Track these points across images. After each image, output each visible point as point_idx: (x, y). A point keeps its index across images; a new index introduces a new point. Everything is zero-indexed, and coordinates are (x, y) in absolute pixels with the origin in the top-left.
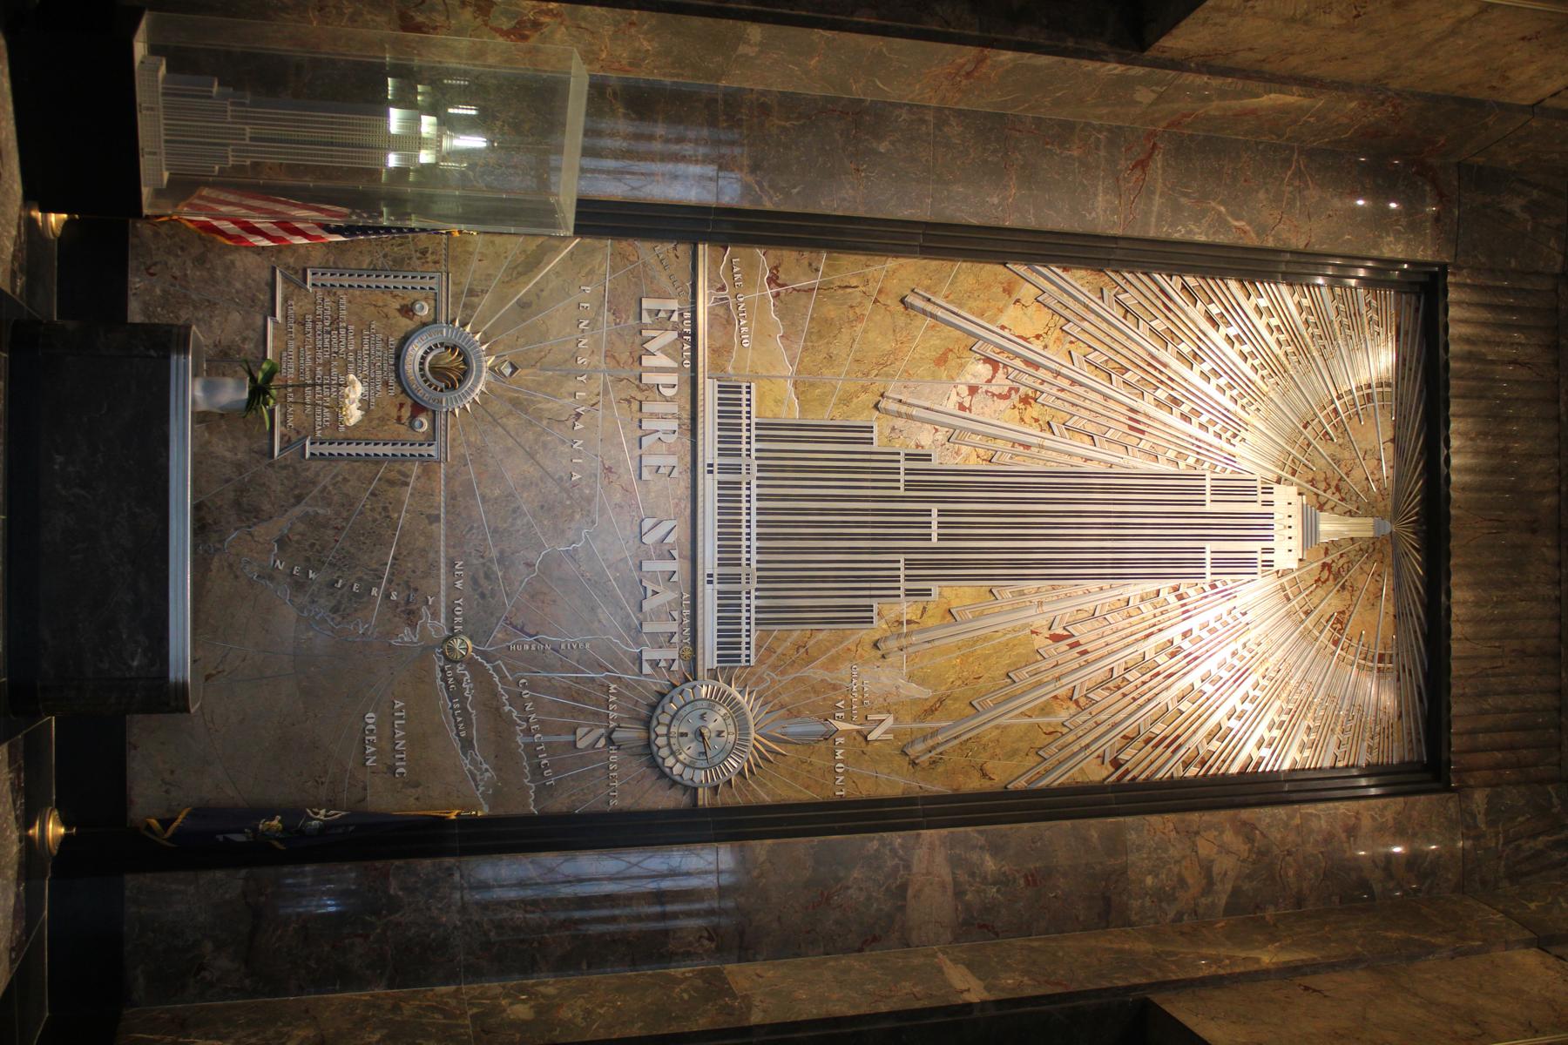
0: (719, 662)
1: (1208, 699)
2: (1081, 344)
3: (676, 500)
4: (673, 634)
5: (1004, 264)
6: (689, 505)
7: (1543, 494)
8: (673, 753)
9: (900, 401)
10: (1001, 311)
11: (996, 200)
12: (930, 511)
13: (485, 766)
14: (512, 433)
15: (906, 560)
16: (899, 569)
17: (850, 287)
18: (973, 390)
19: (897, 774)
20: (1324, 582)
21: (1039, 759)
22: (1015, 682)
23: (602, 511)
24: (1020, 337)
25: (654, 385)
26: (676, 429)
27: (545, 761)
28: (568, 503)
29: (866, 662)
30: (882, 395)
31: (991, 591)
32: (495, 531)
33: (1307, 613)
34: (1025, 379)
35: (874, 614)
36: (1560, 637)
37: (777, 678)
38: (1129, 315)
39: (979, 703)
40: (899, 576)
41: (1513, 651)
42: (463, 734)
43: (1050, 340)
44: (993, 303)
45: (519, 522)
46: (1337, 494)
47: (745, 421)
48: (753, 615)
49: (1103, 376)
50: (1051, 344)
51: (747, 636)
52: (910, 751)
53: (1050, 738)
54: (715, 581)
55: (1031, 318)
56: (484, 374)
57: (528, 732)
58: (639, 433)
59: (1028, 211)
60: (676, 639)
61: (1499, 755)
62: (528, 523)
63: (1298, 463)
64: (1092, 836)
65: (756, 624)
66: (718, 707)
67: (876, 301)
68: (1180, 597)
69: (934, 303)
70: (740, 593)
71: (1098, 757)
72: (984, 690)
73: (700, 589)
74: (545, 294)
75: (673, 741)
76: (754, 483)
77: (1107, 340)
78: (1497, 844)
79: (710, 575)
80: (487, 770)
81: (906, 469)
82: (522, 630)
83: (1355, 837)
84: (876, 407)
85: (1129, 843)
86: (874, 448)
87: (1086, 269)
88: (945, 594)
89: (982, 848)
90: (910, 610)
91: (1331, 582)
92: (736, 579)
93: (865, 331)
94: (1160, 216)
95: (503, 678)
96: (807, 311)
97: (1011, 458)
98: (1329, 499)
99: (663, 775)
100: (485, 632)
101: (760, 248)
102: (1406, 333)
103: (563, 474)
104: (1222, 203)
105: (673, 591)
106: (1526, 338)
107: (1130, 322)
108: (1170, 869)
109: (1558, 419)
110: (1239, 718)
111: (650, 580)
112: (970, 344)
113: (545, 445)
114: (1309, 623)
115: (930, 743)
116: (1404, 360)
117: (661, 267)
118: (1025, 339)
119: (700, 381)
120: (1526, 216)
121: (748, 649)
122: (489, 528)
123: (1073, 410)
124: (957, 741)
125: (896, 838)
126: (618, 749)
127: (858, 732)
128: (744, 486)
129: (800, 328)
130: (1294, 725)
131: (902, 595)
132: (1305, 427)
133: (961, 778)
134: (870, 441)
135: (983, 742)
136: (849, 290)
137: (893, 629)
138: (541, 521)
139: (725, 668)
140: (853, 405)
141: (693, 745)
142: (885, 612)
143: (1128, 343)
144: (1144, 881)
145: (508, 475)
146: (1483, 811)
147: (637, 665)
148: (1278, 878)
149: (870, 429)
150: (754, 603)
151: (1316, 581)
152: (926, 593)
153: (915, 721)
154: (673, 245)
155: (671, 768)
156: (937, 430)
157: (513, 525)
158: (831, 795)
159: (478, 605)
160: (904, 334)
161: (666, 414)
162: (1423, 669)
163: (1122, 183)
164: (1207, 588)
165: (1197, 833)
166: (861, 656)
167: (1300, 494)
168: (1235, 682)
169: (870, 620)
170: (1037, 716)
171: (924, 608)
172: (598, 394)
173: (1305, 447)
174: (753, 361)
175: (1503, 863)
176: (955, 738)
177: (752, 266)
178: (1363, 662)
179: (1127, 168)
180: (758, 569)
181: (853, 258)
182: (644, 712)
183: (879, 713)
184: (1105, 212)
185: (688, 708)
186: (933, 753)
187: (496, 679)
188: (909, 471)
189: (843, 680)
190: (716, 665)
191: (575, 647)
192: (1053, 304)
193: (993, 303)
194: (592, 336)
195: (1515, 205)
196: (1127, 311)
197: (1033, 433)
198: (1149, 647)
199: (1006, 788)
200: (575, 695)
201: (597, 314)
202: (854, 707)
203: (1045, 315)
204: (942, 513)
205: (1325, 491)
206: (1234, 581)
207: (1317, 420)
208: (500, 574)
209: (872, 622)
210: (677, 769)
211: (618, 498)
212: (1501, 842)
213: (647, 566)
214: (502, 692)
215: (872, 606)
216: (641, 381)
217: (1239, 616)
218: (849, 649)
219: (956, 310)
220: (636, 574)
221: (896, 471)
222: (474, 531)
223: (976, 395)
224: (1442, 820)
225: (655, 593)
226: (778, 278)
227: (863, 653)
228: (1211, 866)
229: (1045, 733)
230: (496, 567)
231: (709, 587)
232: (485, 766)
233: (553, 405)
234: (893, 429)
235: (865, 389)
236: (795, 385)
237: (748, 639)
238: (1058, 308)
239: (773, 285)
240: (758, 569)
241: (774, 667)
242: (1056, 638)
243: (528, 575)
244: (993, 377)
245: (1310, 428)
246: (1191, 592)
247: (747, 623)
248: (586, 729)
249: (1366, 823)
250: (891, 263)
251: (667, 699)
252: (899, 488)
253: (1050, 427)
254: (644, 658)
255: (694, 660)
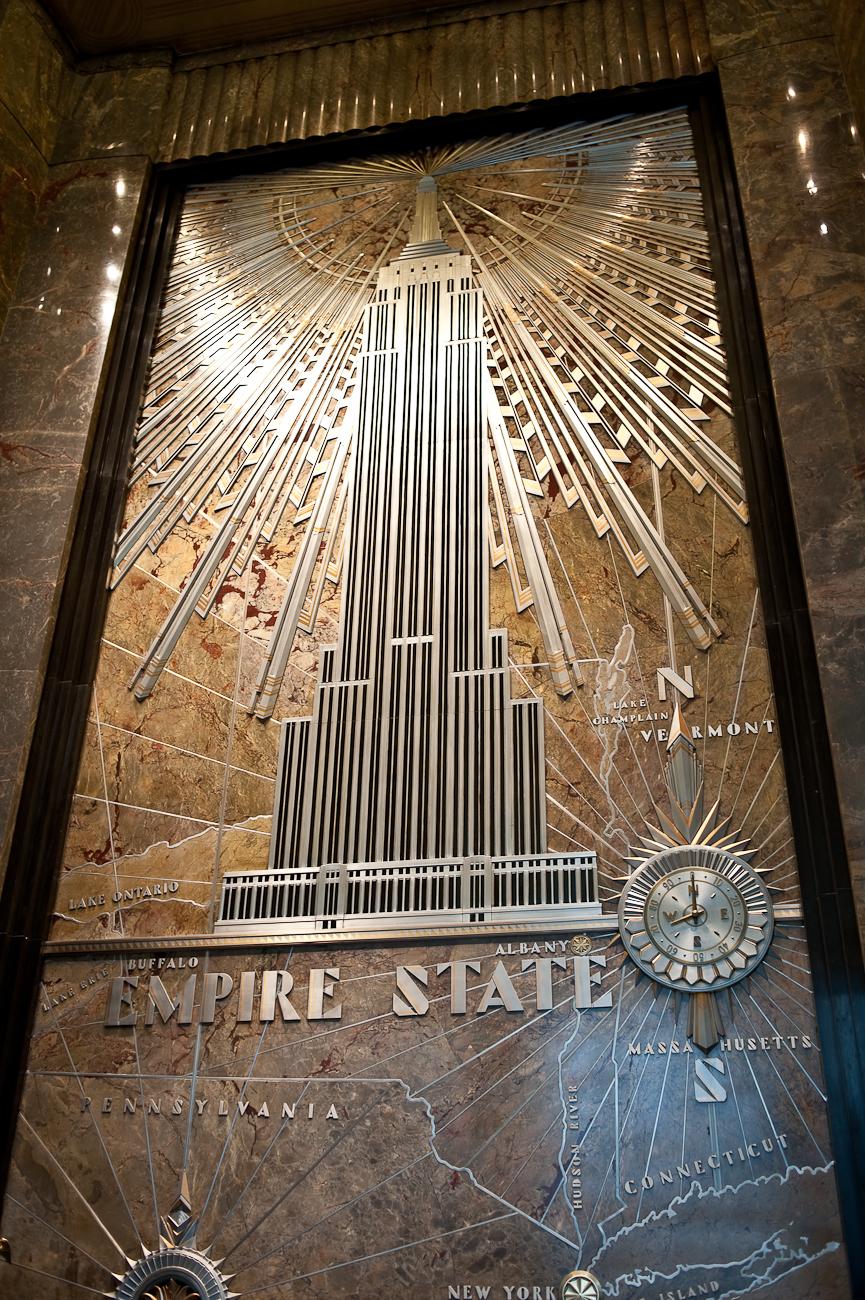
0: (592, 900)
1: (624, 322)
2: (209, 501)
3: (371, 969)
4: (556, 967)
5: (110, 591)
6: (378, 951)
7: (391, 49)
8: (726, 957)
9: (259, 694)
10: (163, 590)
11: (27, 598)
12: (394, 647)
13: (764, 1248)
14: (269, 1209)
15: (455, 670)
16: (467, 678)
17: (119, 763)
18: (252, 612)
19: (737, 656)
20: (487, 229)
21: (708, 493)
22: (610, 530)
23: (383, 1073)
24: (194, 568)
25: (217, 1006)
26: (276, 972)
27: (750, 1151)
28: (368, 1123)
29: (590, 709)
30: (250, 715)
31: (496, 568)
32: (405, 1233)
33: (522, 240)
34: (242, 556)
35: (525, 702)
36: (542, 9)
37: (613, 817)
38: (180, 456)
39: (638, 568)
40: (476, 677)
41: (557, 43)
42: (715, 1286)
43: (201, 533)
44: (154, 600)
45: (393, 1197)
46: (389, 231)
47: (272, 882)
48: (528, 856)
49: (247, 476)
50: (205, 533)
51: (555, 863)
52: (705, 644)
53: (680, 482)
54: (480, 910)
55: (175, 557)
56: (184, 1253)
57: (706, 1178)
58: (279, 1024)
59: (43, 563)
60: (561, 961)
61: (673, 37)
62: (395, 1183)
63: (354, 271)
64: (798, 410)
65: (539, 852)
66: (655, 897)
67: (138, 731)
68: (503, 365)
69: (147, 664)
70: (496, 877)
71: (700, 427)
72: (621, 564)
73: (491, 931)
74: (86, 1163)
75: (708, 958)
76: (351, 866)
77: (206, 474)
78: (772, 16)
79: (473, 918)
80: (770, 1245)
81: (342, 680)
82: (551, 1190)
83: (775, 144)
84: (264, 721)
85: (803, 369)
86: (313, 719)
87: (125, 505)
88: (499, 621)
89: (825, 535)
90: (520, 661)
91: (487, 223)
92: (477, 883)
93: (172, 741)
94: (67, 428)
95: (624, 1220)
96: (141, 812)
97: (334, 562)
98: (396, 238)
99: (757, 972)
100: (555, 1249)
101: (59, 876)
102: (225, 194)
103: (329, 1131)
104: (59, 369)
105: (493, 968)
106: (233, 87)
107: (188, 453)
108: (833, 320)
109: (315, 49)
110: (646, 287)
111: (478, 1001)
112: (198, 620)
113: (288, 1159)
114: (530, 238)
115: (693, 619)
116: (252, 192)
117: (68, 1002)
118: (198, 560)
119: (215, 943)
120: (109, 103)
121: (573, 861)
122: (400, 1243)
123: (283, 501)
124: (690, 589)
125: (822, 640)
126: (724, 1037)
127: (683, 709)
128: (354, 879)
129: (162, 820)
130: (652, 233)
131: (501, 671)
132: (316, 270)
133: (738, 579)
134: (306, 726)
135: (690, 558)
136: (122, 764)
137: (545, 678)
138: (393, 1163)
139: (600, 890)
140: (260, 749)
141: (712, 928)
142: (523, 691)
143: (211, 453)
144: (851, 345)
145: (325, 1213)
146: (735, 36)
147: (600, 1014)
148: (834, 209)
149: (291, 727)
150: (510, 856)
151: (486, 236)
152: (497, 643)
153: (666, 642)
154: (44, 987)
155: (748, 958)
156: (297, 648)
157: (396, 1206)
158: (773, 737)
159: (513, 1260)
160: (180, 695)
161: (256, 987)
162: (584, 125)
163: (25, 469)
164: (493, 339)
165: (784, 299)
166: (581, 714)
167: (388, 265)
168: (602, 297)
169: (533, 709)
170: (652, 500)
171: (517, 643)
172: (224, 1082)
173: (337, 267)
174: (196, 878)
175: (794, 7)
176: (685, 591)
177: (80, 885)
178: (576, 180)
179: (10, 465)
180: (465, 854)
181: (84, 762)
182: (667, 1001)
183: (656, 686)
184: (54, 483)
185: (659, 939)
186: (709, 617)
187: (627, 1229)
188: (345, 676)
189: (612, 736)
190: (596, 903)
191: (575, 1108)
192: (160, 535)
193: (154, 600)
194: (146, 1094)
195: (96, 113)
196: (176, 458)
197: (307, 543)
198: (562, 392)
199: (746, 525)
200: (646, 1105)
201: (119, 1086)
202: (649, 717)
203: (174, 543)
204: (397, 633)
205: (387, 242)
206: (485, 314)
207: (309, 260)
208: (468, 1226)
209: (536, 705)
210: (748, 949)
211: (364, 1051)
212: (770, 13)
213: (459, 1004)
214: (646, 1220)
215: (515, 706)
216: (211, 1024)
217: (525, 304)
218: (572, 730)
219: (157, 639)
220: (470, 1022)
221: (344, 691)
222: (404, 1266)
223: (258, 608)
224: (749, 69)
225: (496, 993)
226: (98, 851)
227: (576, 712)
228: (825, 278)
229: (674, 488)
230: (459, 1232)
231: (488, 919)
232: (764, 1248)
233: (234, 1146)
234: (292, 699)
235: (242, 737)
236: (229, 822)
237: (560, 862)
238: (165, 529)
239: (107, 857)
240: (465, 854)
241: (598, 825)
242: (554, 489)
243: (471, 1182)
244: (238, 591)
245: (317, 266)
246: (497, 355)
247: (538, 864)
248: (698, 1087)
249: (758, 136)
250: (96, 717)
251: (647, 969)
252: (365, 687)
253: (300, 523)
254: (590, 1006)
255: (590, 933)
